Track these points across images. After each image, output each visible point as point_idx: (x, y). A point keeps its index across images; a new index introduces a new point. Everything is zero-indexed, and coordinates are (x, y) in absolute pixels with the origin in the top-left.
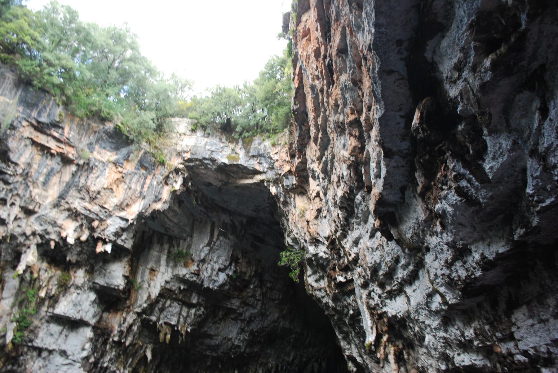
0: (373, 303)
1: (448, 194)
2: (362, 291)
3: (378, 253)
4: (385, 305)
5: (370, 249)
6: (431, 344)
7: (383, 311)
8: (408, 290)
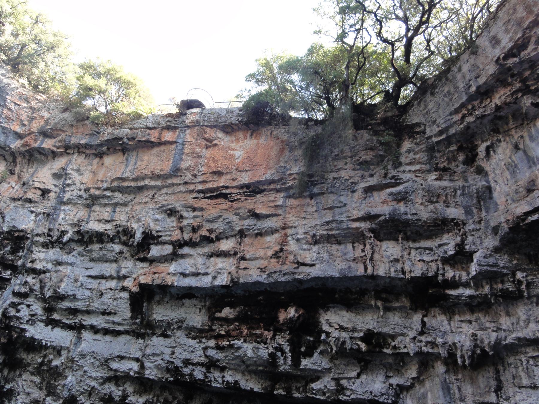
0: (12, 312)
1: (261, 349)
2: (11, 296)
3: (88, 293)
4: (31, 325)
5: (79, 284)
6: (71, 384)
7: (22, 326)
8: (87, 335)
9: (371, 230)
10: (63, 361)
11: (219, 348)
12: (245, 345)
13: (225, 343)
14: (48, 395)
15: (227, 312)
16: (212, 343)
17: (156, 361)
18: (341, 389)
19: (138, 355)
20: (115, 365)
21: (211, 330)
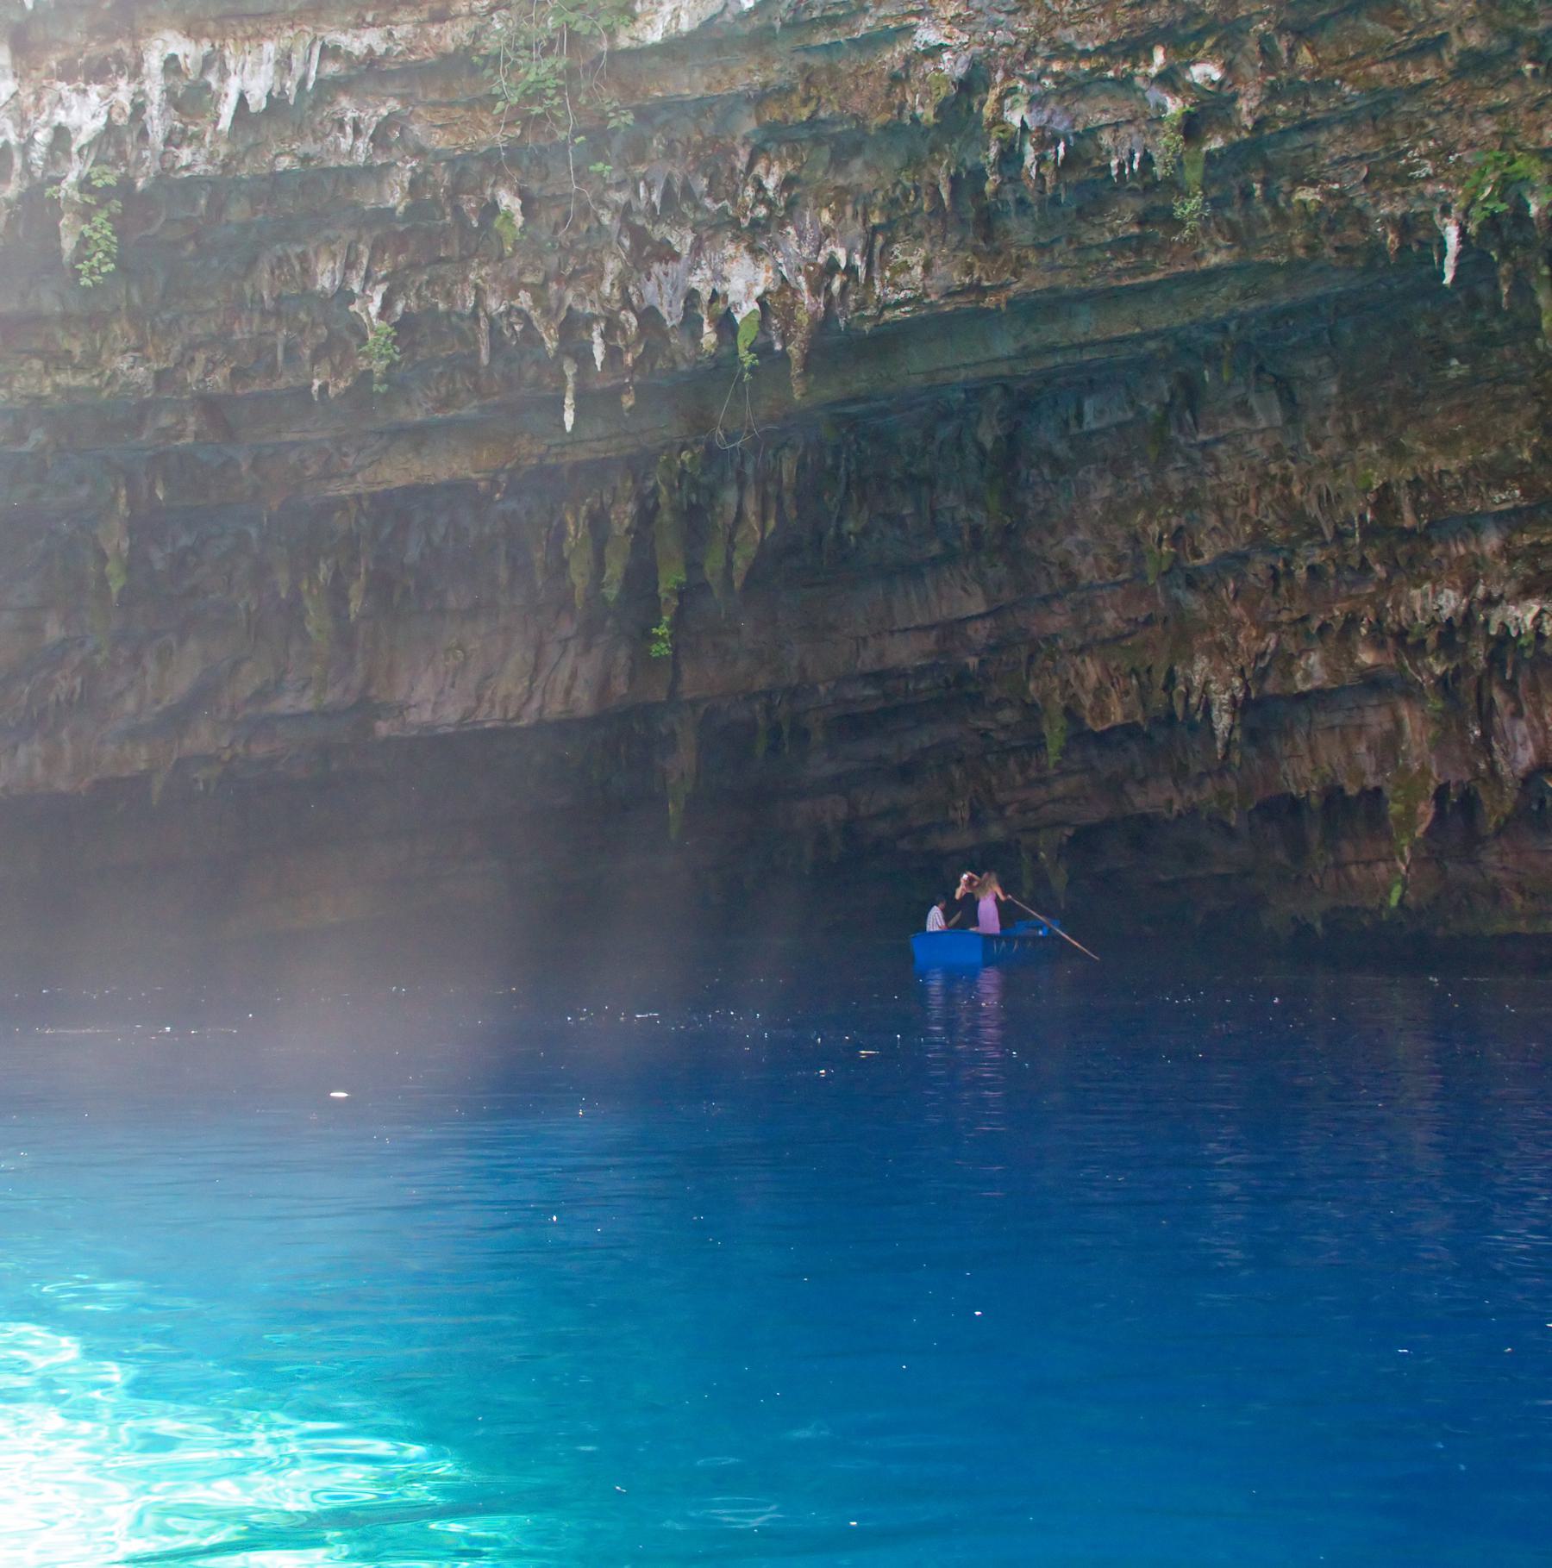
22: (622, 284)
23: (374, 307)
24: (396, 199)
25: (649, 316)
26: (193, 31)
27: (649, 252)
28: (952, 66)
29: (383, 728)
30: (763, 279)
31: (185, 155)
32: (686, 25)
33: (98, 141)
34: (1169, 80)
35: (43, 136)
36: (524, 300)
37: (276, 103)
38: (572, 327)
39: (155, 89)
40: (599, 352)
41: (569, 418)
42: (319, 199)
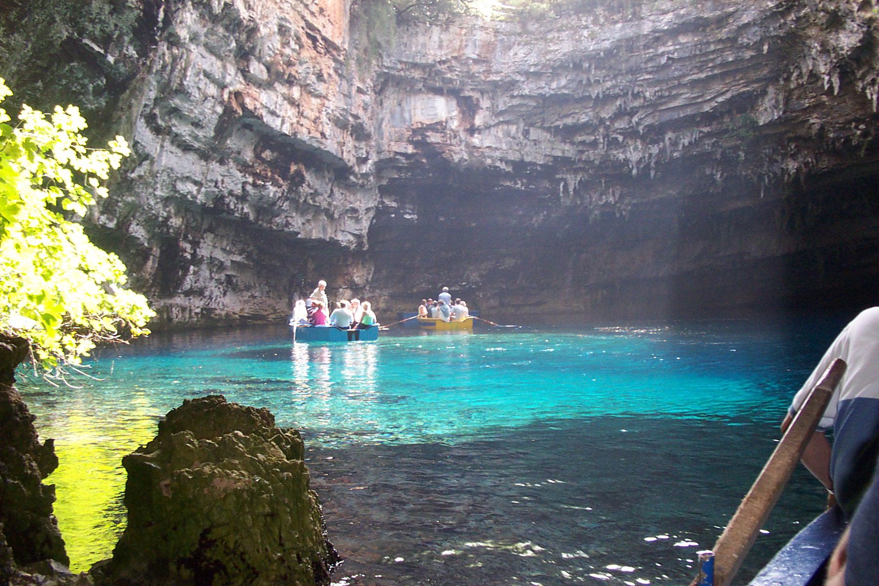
9: (352, 126)
10: (142, 173)
11: (254, 185)
12: (271, 188)
13: (260, 182)
14: (102, 213)
15: (267, 154)
16: (250, 180)
17: (210, 187)
18: (288, 224)
19: (198, 178)
20: (180, 186)
21: (253, 166)
22: (768, 167)
23: (719, 176)
24: (718, 156)
25: (775, 174)
26: (674, 132)
27: (772, 161)
28: (817, 127)
29: (746, 257)
30: (796, 165)
31: (675, 154)
32: (767, 121)
33: (657, 155)
34: (857, 128)
35: (647, 155)
36: (749, 172)
37: (690, 143)
38: (761, 177)
39: (667, 142)
40: (766, 181)
41: (762, 195)
42: (705, 158)
